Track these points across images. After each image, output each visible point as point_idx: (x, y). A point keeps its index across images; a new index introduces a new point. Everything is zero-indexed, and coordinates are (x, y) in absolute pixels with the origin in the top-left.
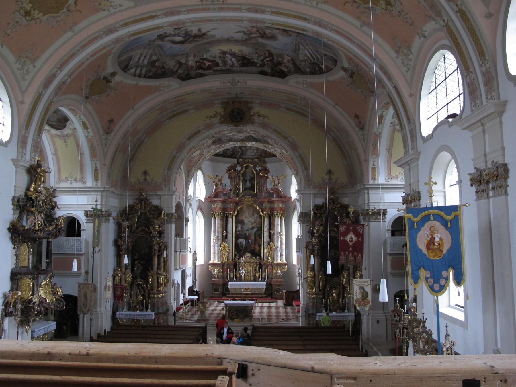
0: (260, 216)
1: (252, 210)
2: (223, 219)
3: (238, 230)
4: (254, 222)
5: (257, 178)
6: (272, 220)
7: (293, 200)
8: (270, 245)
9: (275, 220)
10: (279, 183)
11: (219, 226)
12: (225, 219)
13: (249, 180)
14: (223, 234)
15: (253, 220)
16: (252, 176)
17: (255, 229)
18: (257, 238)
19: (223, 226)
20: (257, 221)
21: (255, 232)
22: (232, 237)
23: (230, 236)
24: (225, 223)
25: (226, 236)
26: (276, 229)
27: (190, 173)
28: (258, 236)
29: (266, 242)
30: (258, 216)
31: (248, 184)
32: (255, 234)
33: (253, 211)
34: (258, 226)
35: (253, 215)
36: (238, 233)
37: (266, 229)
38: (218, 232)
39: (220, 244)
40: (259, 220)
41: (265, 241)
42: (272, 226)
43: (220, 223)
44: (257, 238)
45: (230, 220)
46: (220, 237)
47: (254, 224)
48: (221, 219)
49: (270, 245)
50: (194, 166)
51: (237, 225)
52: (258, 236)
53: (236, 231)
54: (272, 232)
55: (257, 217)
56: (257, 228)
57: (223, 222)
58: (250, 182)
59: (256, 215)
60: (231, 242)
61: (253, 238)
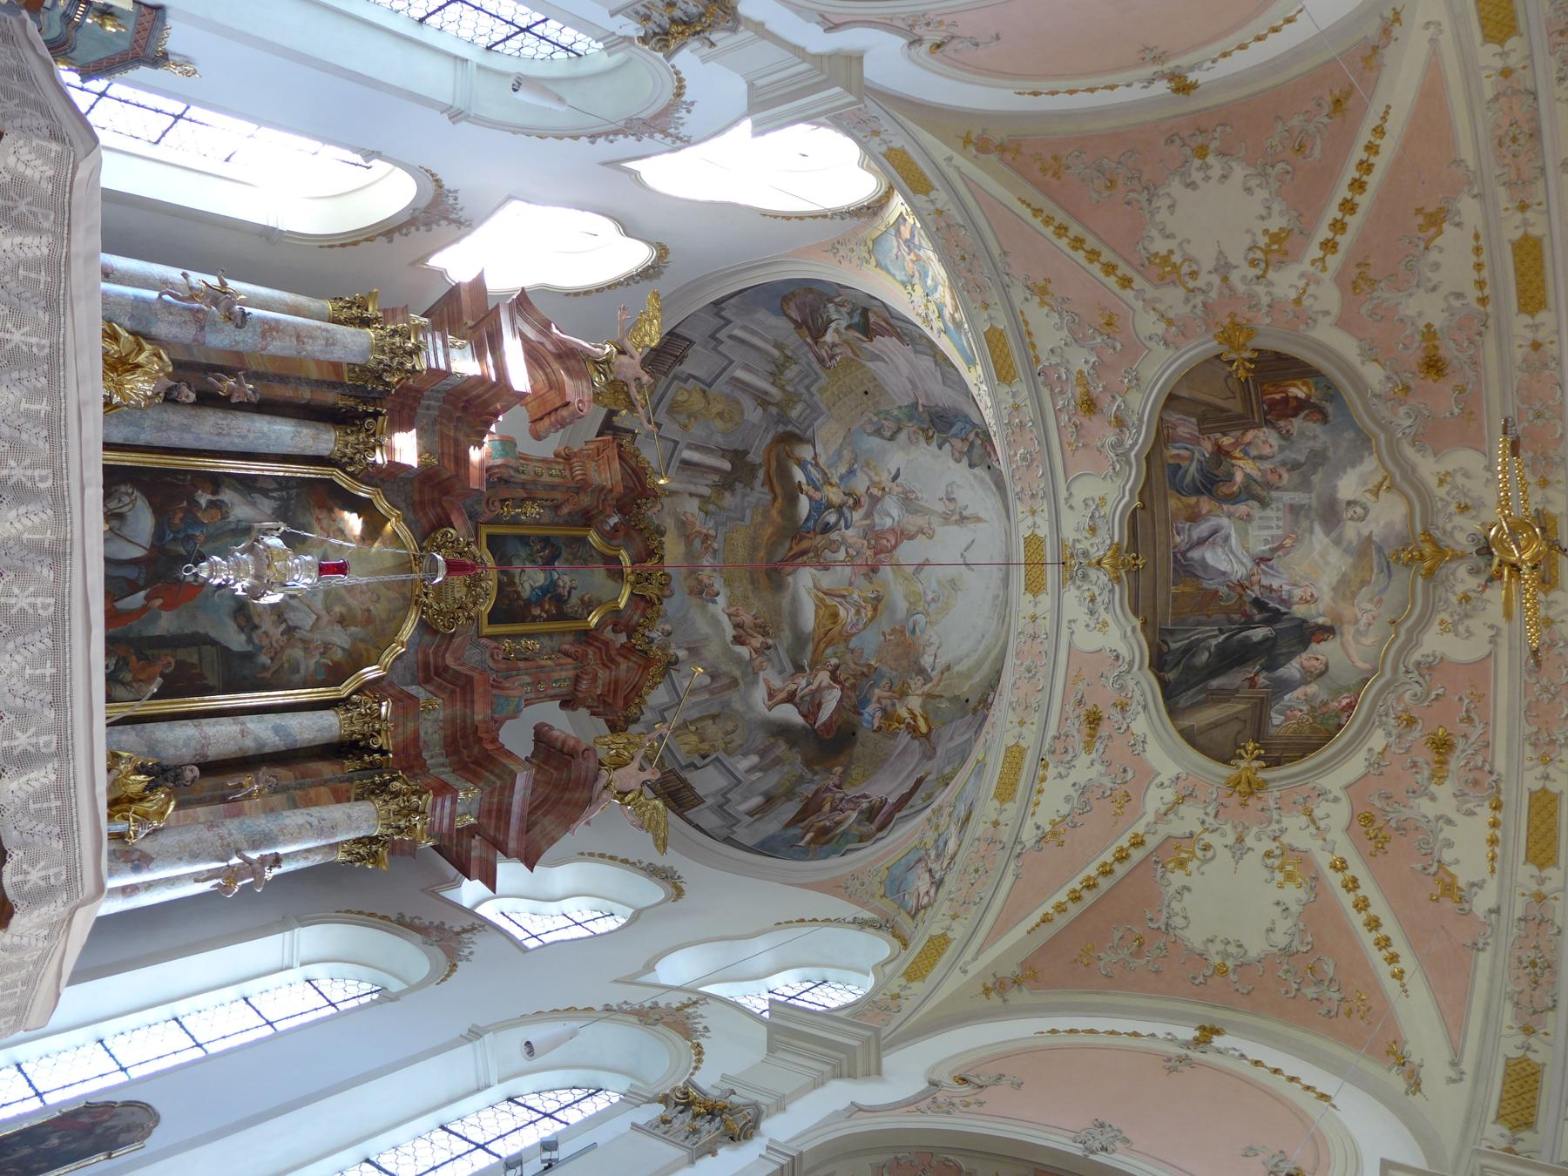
0: (335, 675)
1: (380, 609)
2: (332, 385)
3: (227, 496)
4: (290, 630)
5: (564, 633)
6: (327, 769)
7: (450, 894)
8: (151, 787)
9: (340, 797)
10: (622, 794)
11: (315, 348)
12: (330, 397)
13: (554, 584)
14: (230, 372)
15: (309, 622)
16: (574, 600)
17: (236, 641)
18: (168, 661)
19: (282, 379)
20: (297, 653)
21: (214, 643)
22: (188, 441)
23: (209, 428)
24: (306, 394)
25: (209, 400)
26: (295, 818)
27: (994, 157)
28: (180, 664)
29: (152, 748)
30: (338, 655)
31: (531, 578)
32: (200, 641)
33: (369, 618)
34: (264, 659)
35: (342, 621)
36: (203, 499)
37: (263, 733)
38: (270, 328)
39: (161, 329)
40: (309, 663)
41: (161, 731)
42: (285, 774)
43: (337, 354)
44: (168, 661)
45: (324, 440)
46: (222, 339)
47: (276, 632)
48: (336, 366)
49: (151, 787)
50: (1039, 200)
51: (265, 493)
52: (180, 664)
53: (216, 481)
54: (251, 782)
55: (327, 647)
56: (247, 657)
57: (319, 383)
58: (545, 590)
59: (340, 639)
60: (145, 438)
61: (166, 623)
